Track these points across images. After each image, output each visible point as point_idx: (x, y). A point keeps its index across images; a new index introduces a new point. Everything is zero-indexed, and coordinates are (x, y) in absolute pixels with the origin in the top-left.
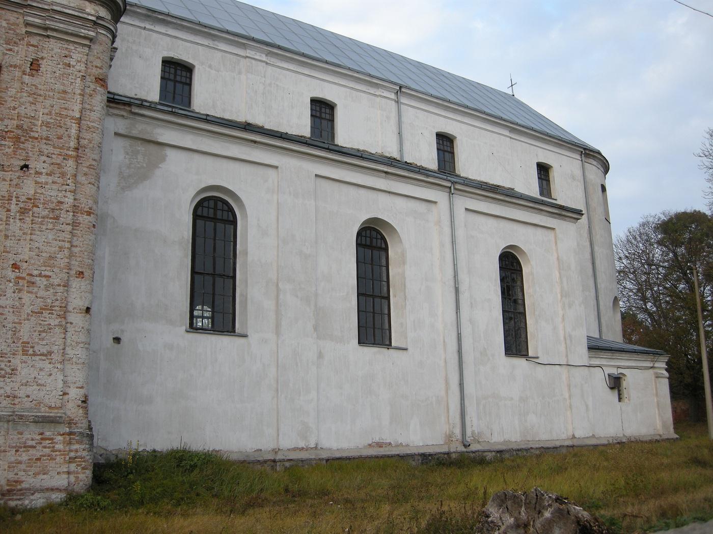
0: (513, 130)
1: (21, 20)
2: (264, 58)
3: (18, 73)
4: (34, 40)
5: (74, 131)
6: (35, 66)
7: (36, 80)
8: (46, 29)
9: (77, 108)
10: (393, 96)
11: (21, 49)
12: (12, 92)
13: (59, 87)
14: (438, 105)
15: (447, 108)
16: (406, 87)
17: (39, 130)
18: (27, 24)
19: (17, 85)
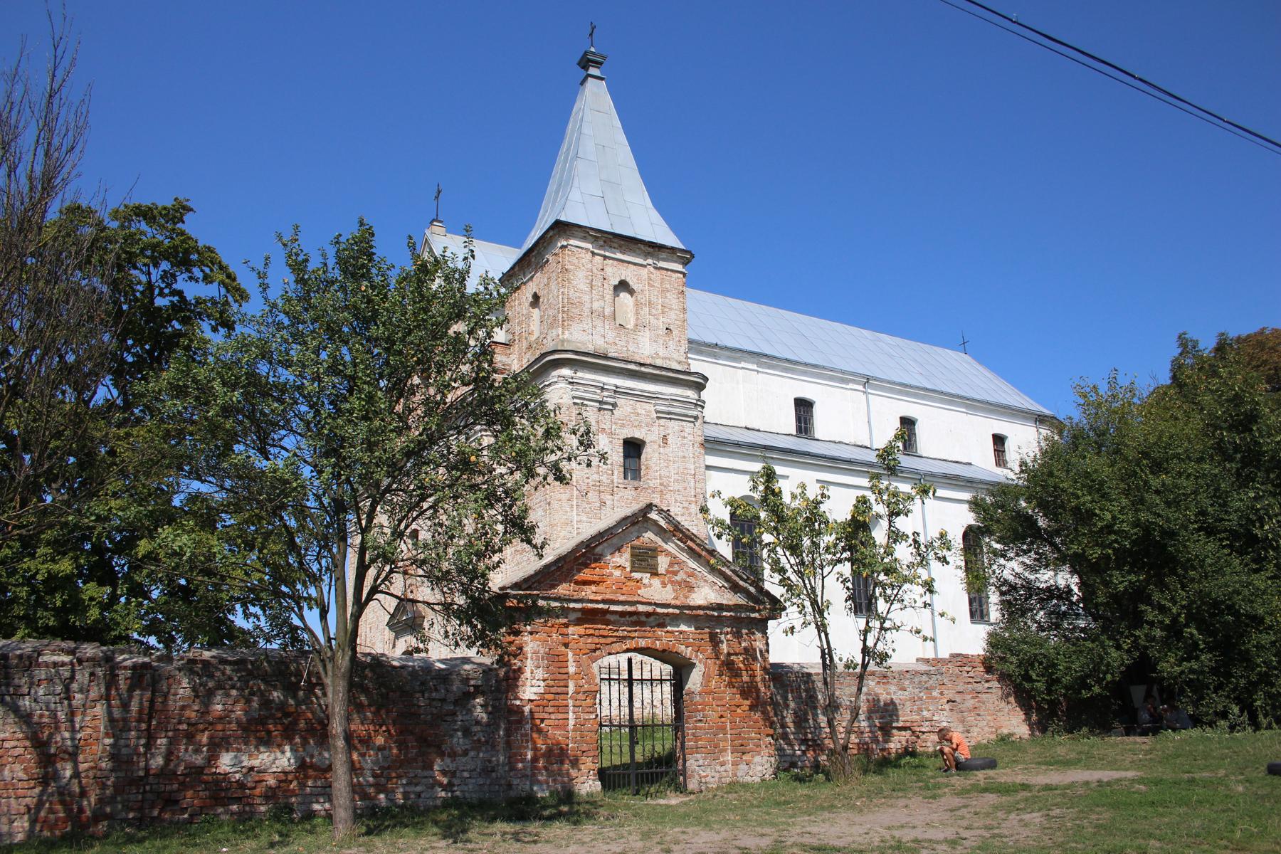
0: (967, 406)
1: (653, 409)
2: (755, 367)
3: (656, 447)
4: (662, 422)
5: (692, 484)
6: (665, 438)
7: (668, 450)
8: (669, 413)
9: (692, 467)
10: (861, 388)
11: (655, 429)
12: (654, 460)
13: (681, 454)
14: (900, 392)
15: (908, 394)
16: (875, 379)
17: (673, 486)
18: (657, 412)
19: (657, 455)
